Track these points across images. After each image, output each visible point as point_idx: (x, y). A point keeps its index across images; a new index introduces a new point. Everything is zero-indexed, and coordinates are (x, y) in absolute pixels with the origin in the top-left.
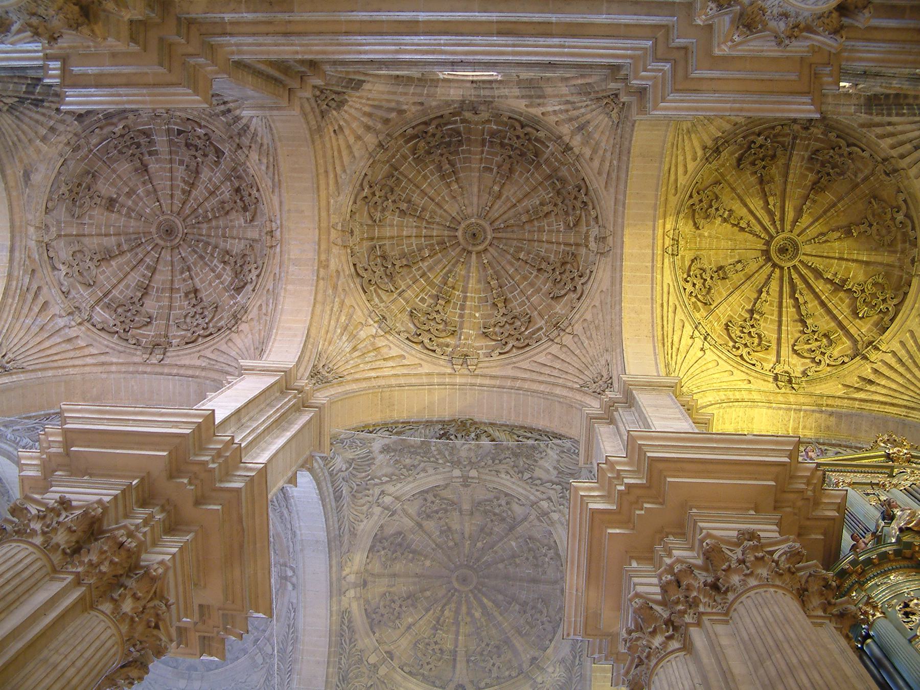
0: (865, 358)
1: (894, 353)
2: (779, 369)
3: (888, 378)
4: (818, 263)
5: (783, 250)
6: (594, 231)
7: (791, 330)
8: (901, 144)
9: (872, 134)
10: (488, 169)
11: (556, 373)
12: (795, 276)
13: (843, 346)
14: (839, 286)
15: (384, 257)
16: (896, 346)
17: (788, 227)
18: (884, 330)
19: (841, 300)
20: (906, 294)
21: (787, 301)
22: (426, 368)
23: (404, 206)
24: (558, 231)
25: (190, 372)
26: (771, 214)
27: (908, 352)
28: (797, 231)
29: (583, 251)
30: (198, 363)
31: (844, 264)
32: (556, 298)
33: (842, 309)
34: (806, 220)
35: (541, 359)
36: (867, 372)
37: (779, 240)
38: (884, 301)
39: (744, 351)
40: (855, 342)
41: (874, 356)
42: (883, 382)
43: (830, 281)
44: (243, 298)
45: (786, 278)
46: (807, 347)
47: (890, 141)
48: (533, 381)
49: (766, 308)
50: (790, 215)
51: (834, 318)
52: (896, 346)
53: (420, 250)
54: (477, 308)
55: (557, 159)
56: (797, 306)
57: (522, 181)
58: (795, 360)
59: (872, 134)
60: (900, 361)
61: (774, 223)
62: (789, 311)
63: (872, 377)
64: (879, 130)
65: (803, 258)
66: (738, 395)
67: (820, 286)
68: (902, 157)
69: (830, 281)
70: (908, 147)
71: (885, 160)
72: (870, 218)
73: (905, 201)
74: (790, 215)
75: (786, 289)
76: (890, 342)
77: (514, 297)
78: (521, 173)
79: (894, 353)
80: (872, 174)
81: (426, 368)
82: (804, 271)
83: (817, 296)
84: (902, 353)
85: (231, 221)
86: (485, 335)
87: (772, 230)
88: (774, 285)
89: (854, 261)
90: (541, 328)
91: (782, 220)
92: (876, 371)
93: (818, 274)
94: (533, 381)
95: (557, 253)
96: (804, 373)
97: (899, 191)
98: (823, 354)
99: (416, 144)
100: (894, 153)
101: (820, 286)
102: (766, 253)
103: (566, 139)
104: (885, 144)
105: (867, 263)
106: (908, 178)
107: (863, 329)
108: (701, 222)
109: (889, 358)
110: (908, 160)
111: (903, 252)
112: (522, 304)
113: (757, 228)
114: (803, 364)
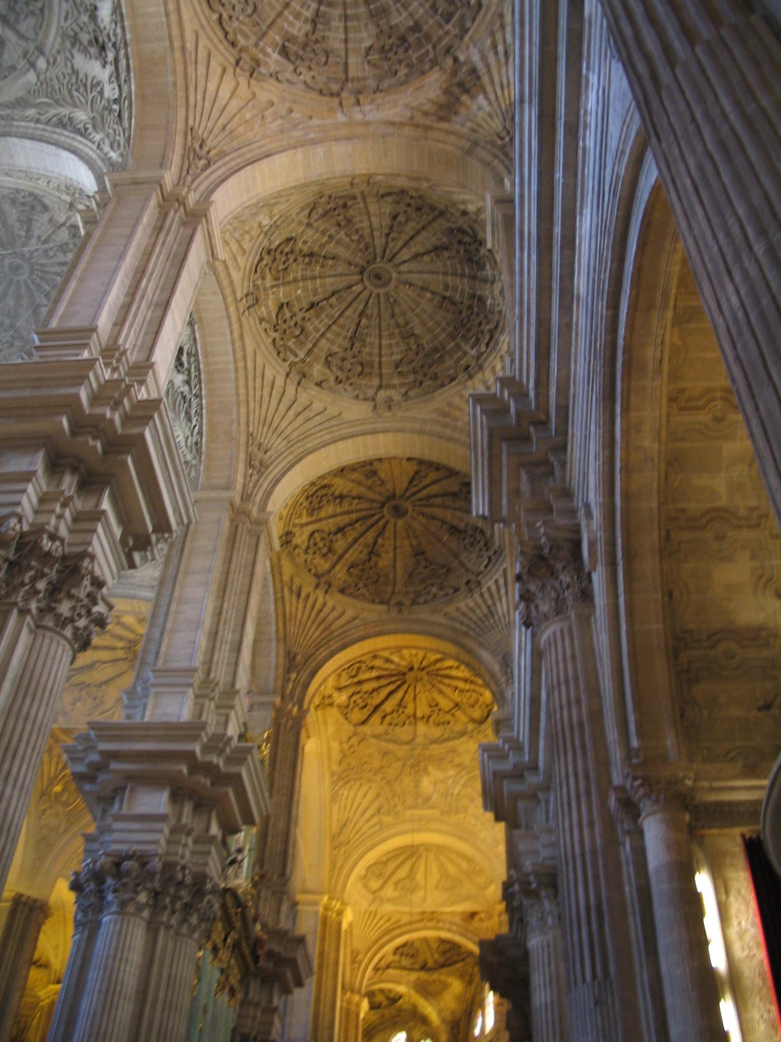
0: (317, 586)
1: (324, 605)
2: (297, 531)
3: (305, 607)
4: (389, 532)
6: (395, 395)
7: (329, 525)
8: (491, 596)
9: (499, 575)
10: (446, 287)
11: (258, 393)
12: (376, 517)
13: (323, 565)
14: (373, 551)
15: (345, 206)
16: (330, 604)
18: (342, 591)
19: (361, 552)
20: (373, 601)
21: (354, 516)
22: (236, 276)
23: (401, 218)
24: (392, 354)
25: (175, 32)
26: (429, 497)
27: (328, 615)
29: (376, 382)
30: (189, 36)
31: (391, 548)
32: (327, 363)
33: (353, 555)
34: (423, 520)
35: (269, 375)
37: (407, 505)
38: (365, 586)
39: (306, 504)
40: (329, 571)
41: (320, 593)
42: (301, 606)
43: (375, 543)
44: (277, 62)
45: (373, 512)
46: (318, 539)
47: (494, 589)
48: (246, 377)
50: (428, 511)
51: (346, 551)
52: (330, 604)
53: (357, 231)
54: (305, 290)
55: (460, 359)
56: (351, 524)
57: (437, 318)
59: (499, 575)
60: (320, 611)
61: (421, 500)
62: (346, 519)
64: (501, 582)
67: (370, 536)
68: (482, 595)
69: (375, 543)
70: (490, 602)
71: (479, 583)
72: (432, 567)
73: (446, 595)
74: (428, 511)
75: (364, 513)
76: (334, 600)
77: (322, 320)
78: (445, 318)
79: (324, 605)
80: (467, 570)
81: (236, 276)
82: (381, 523)
83: (362, 535)
84: (326, 611)
85: (366, 25)
86: (281, 307)
88: (364, 505)
89: (395, 556)
90: (296, 355)
91: (422, 506)
92: (308, 596)
93: (380, 534)
94: (246, 377)
95: (370, 354)
96: (296, 546)
97: (457, 590)
98: (315, 553)
99: (468, 234)
100: (484, 589)
102: (393, 496)
103: (480, 375)
104: (491, 583)
105: (394, 567)
106: (465, 598)
107: (340, 574)
109: (320, 601)
110: (479, 600)
111: (407, 593)
112: (317, 330)
114: (303, 542)
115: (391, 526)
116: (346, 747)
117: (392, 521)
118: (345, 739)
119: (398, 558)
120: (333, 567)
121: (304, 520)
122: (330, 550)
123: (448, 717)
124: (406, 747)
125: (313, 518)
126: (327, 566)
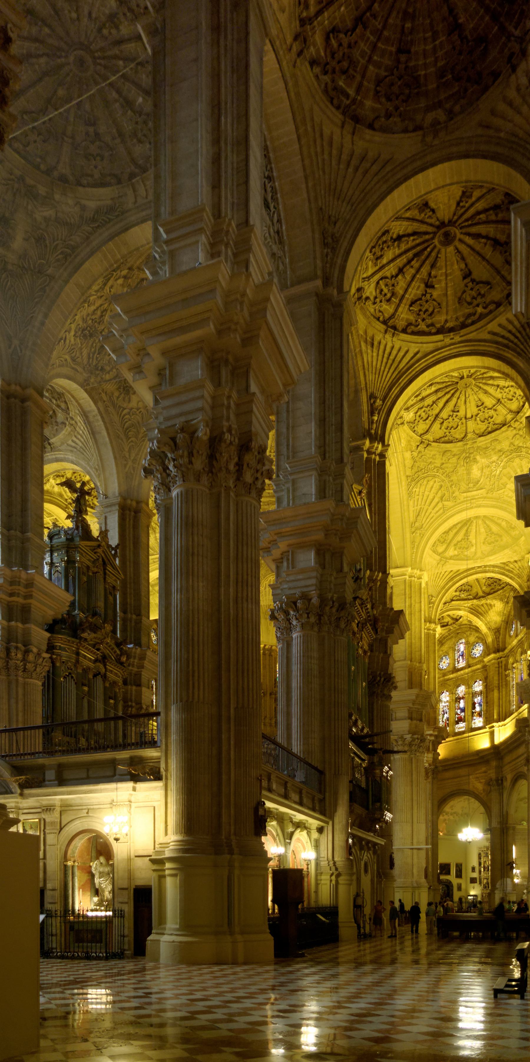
5: (446, 235)
13: (388, 309)
28: (462, 237)
61: (467, 220)
63: (376, 343)
82: (433, 254)
89: (446, 284)
98: (381, 301)
105: (446, 295)
115: (442, 255)
116: (415, 454)
117: (443, 250)
118: (414, 448)
119: (449, 285)
120: (396, 310)
121: (370, 272)
122: (393, 294)
123: (492, 412)
124: (460, 444)
125: (377, 268)
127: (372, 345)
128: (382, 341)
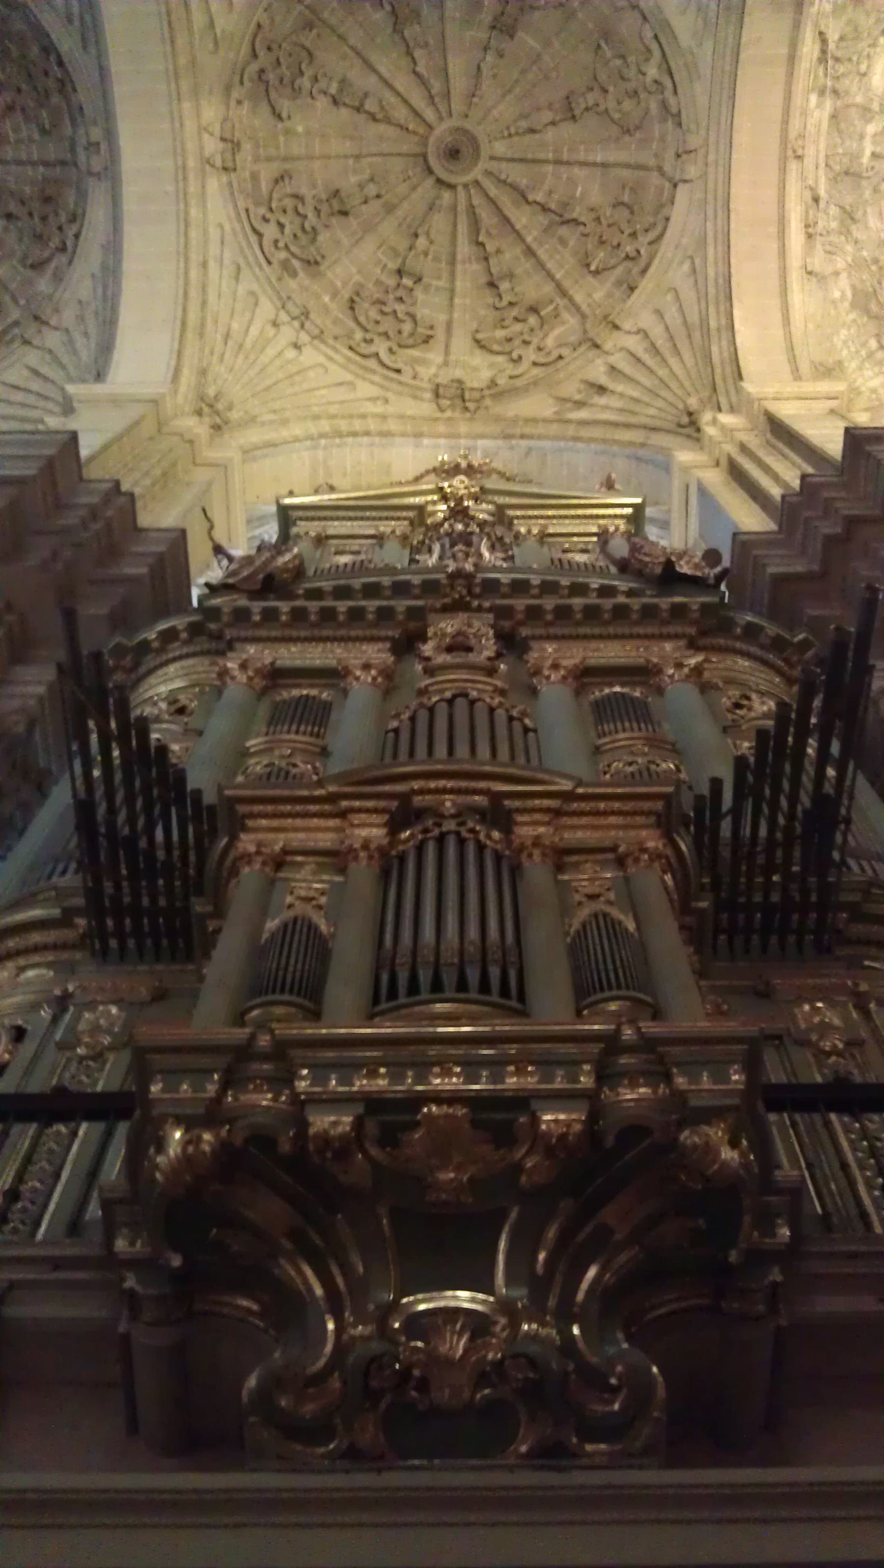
1: (643, 333)
4: (517, 174)
5: (453, 154)
11: (31, 399)
16: (647, 320)
17: (457, 106)
21: (464, 248)
24: (31, 140)
32: (38, 266)
36: (598, 372)
46: (500, 334)
49: (426, 266)
51: (550, 276)
52: (647, 320)
58: (479, 359)
65: (494, 166)
66: (358, 425)
67: (521, 218)
74: (459, 84)
75: (463, 228)
84: (657, 333)
87: (429, 114)
92: (613, 369)
101: (521, 218)
108: (285, 106)
109: (633, 343)
113: (401, 114)
114: (491, 366)
119: (582, 157)
126: (571, 321)
127: (602, 389)
128: (612, 359)
